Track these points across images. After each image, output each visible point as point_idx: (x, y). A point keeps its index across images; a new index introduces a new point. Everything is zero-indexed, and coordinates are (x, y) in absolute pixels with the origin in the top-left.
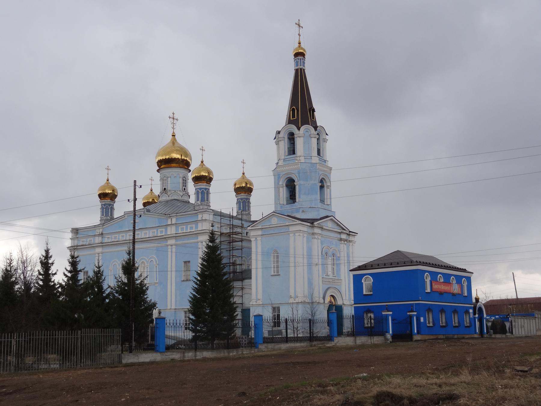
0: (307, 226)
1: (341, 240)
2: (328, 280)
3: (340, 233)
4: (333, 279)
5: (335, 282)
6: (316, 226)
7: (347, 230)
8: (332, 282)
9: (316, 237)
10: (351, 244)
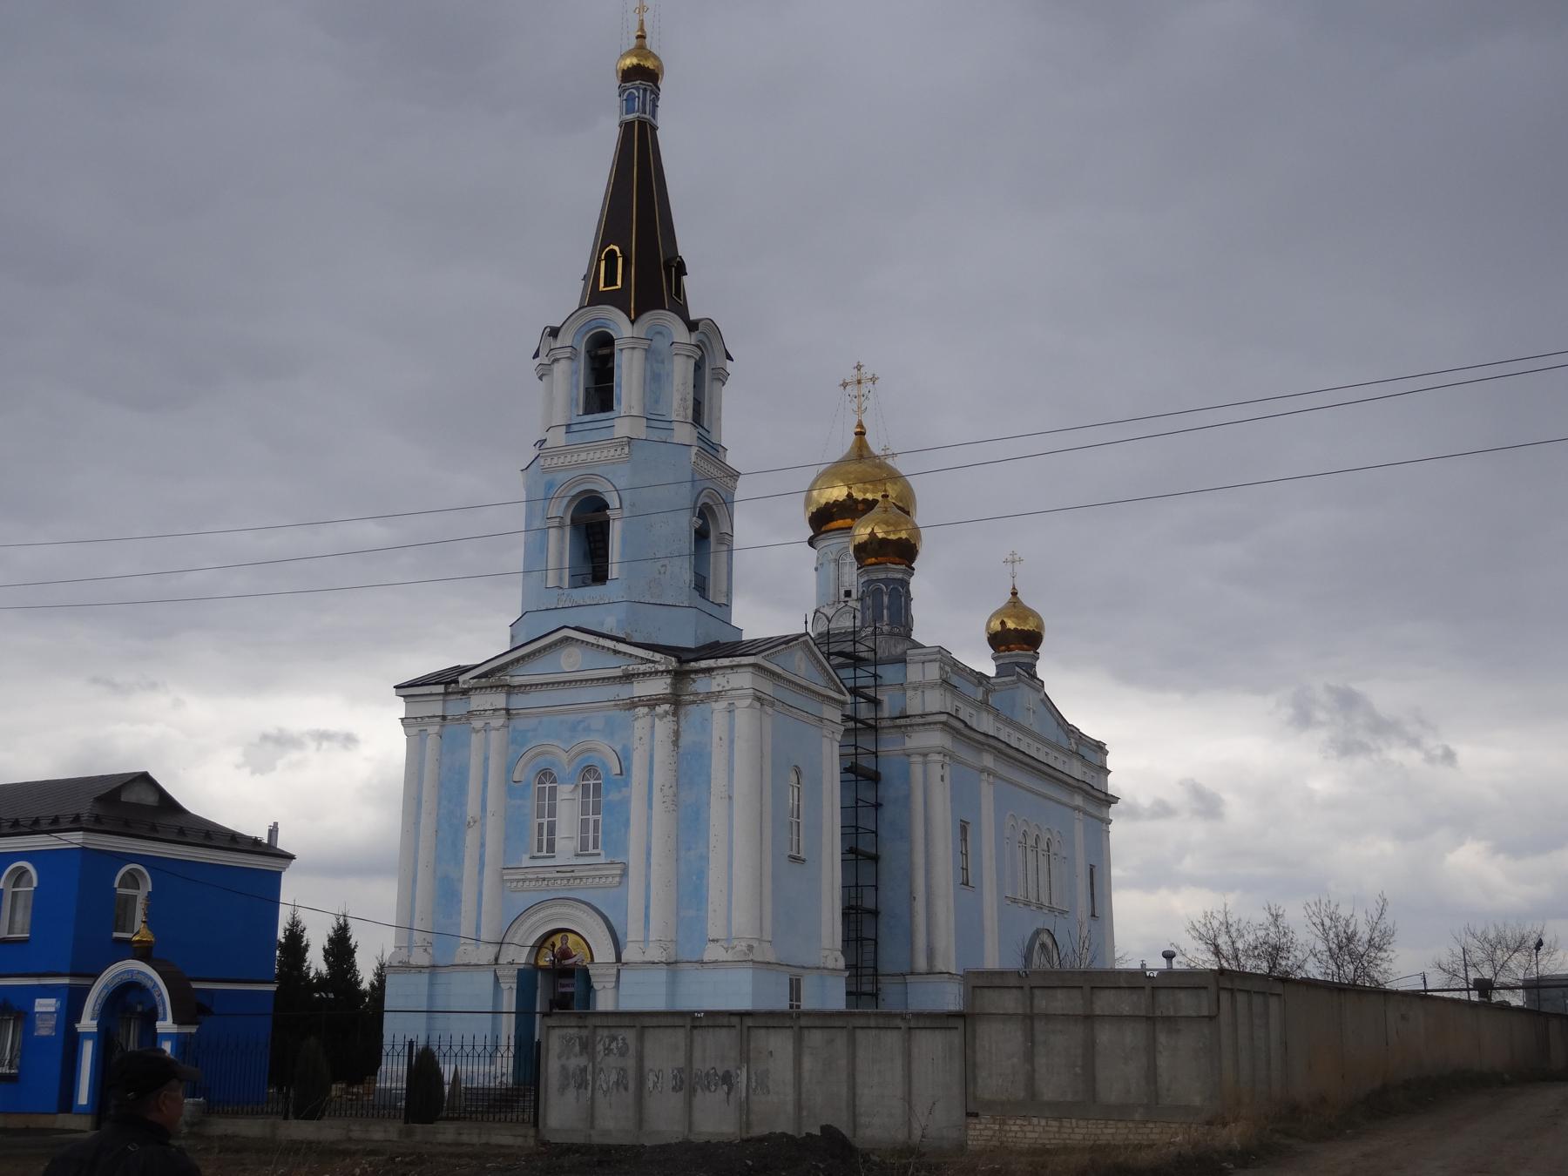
0: (441, 697)
1: (633, 704)
2: (532, 873)
3: (628, 678)
4: (558, 869)
5: (575, 878)
6: (466, 686)
7: (657, 657)
8: (555, 879)
9: (477, 723)
10: (720, 706)
